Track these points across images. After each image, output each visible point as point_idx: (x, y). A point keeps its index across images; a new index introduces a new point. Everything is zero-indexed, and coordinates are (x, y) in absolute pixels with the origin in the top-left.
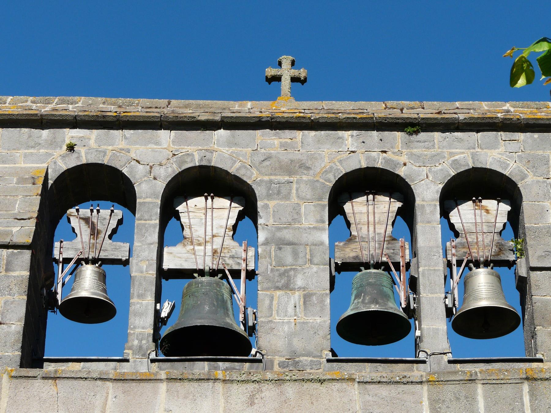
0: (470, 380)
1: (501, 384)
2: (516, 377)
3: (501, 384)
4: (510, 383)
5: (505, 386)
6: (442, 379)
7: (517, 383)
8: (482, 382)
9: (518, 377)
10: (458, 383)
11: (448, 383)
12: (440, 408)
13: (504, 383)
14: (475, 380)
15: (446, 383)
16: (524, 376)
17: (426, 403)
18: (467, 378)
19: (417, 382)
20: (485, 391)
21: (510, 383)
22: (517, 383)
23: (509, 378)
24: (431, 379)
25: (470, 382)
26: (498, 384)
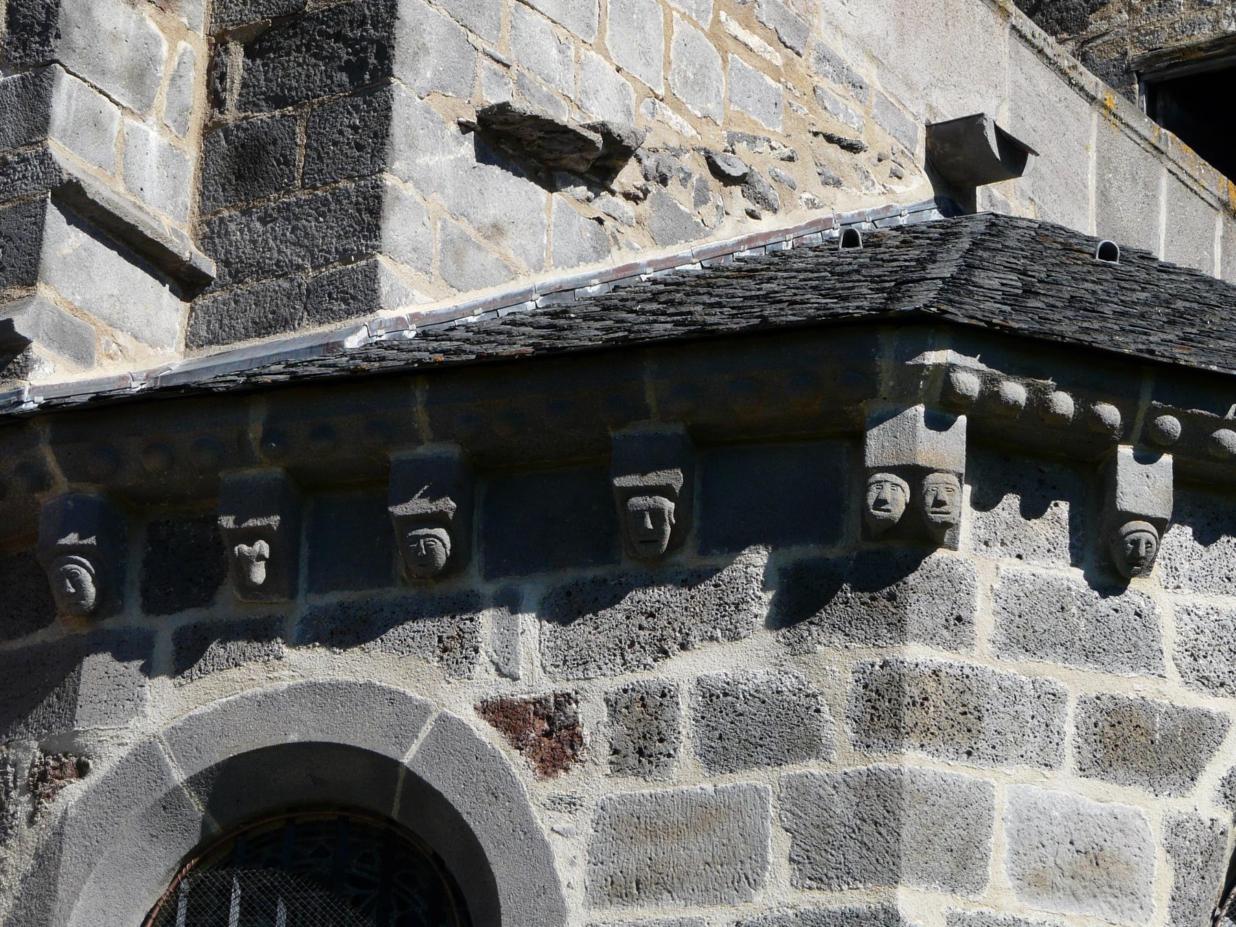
0: (1156, 148)
1: (1192, 190)
2: (1213, 189)
3: (1192, 190)
4: (1203, 199)
5: (1196, 199)
6: (1122, 115)
7: (1212, 206)
8: (1170, 165)
9: (1216, 192)
10: (1139, 141)
11: (1127, 131)
12: (1109, 181)
13: (1196, 193)
14: (1162, 153)
15: (1122, 127)
16: (1225, 198)
17: (1093, 154)
18: (1153, 141)
19: (1087, 95)
20: (1171, 191)
21: (1203, 199)
22: (1212, 206)
23: (1205, 185)
24: (1108, 103)
25: (1155, 152)
26: (1187, 186)
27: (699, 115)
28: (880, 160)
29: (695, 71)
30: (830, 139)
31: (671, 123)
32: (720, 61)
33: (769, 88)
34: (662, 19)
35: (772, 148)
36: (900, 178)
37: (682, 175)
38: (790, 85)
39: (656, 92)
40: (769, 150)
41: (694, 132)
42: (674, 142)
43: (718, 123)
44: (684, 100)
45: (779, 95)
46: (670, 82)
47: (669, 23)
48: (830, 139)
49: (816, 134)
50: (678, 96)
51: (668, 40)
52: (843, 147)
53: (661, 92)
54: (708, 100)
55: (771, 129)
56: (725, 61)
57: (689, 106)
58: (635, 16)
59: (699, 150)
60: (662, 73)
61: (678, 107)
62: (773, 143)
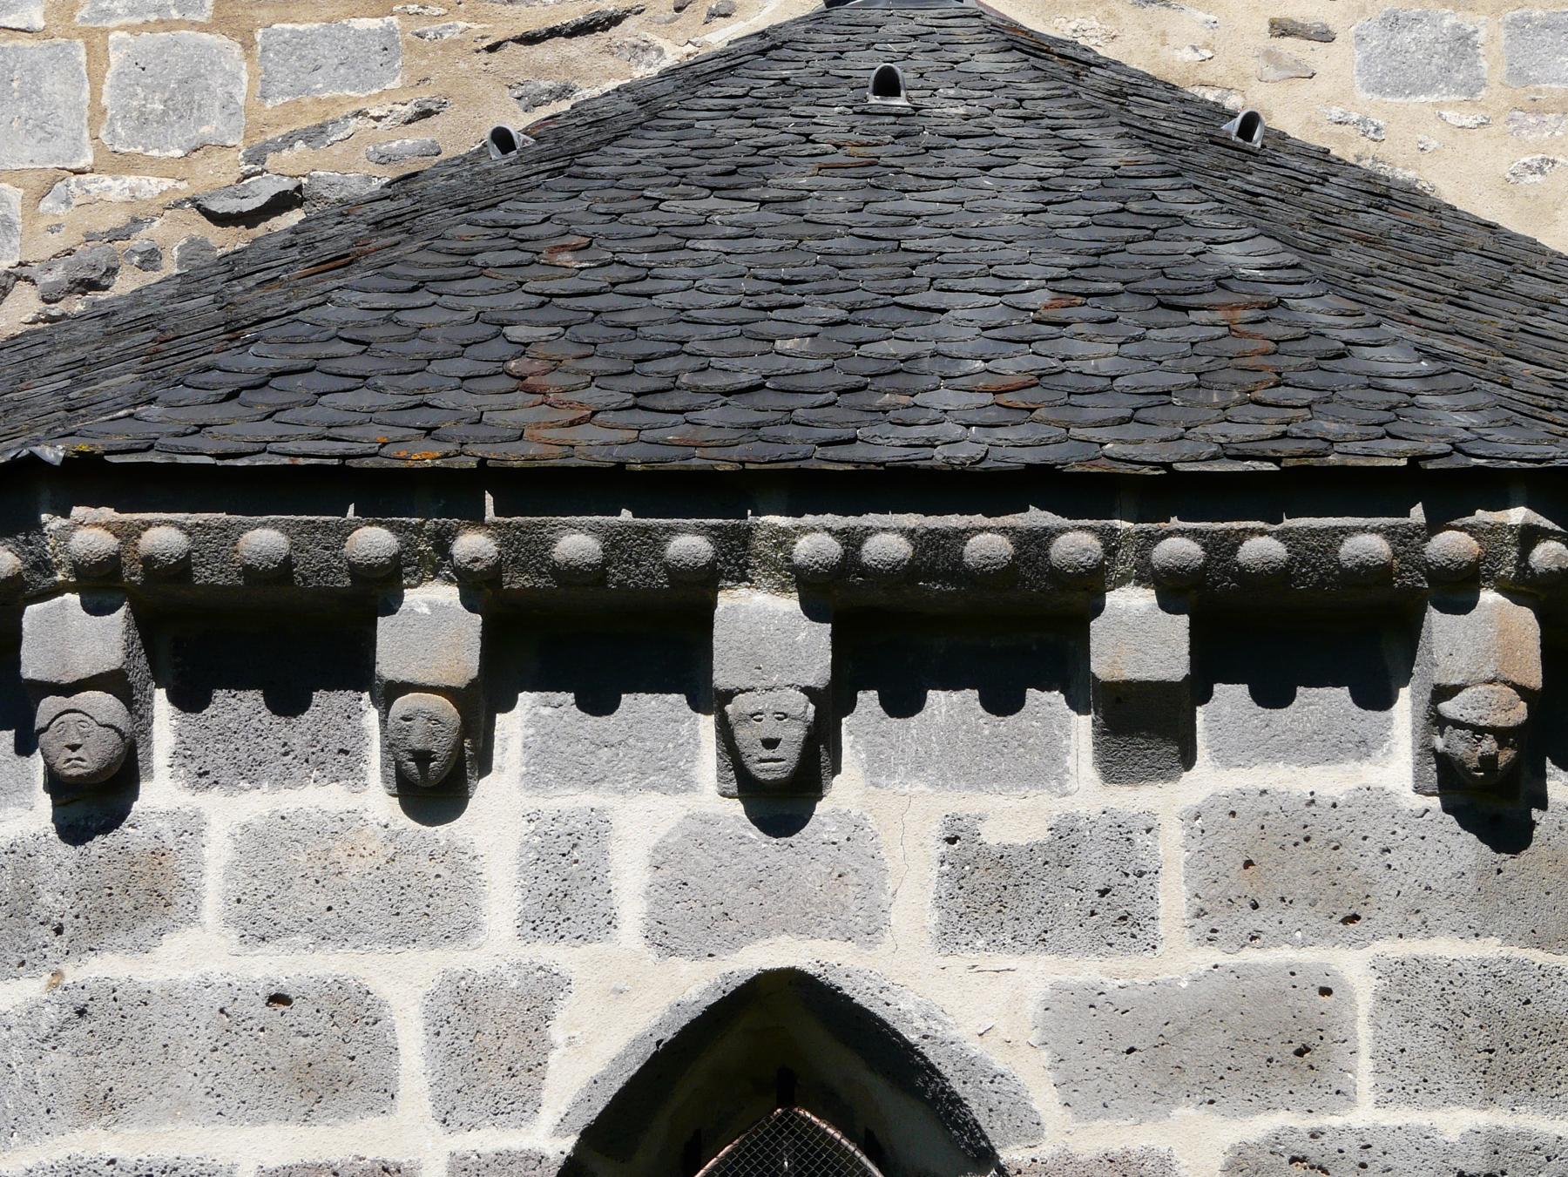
27: (179, 153)
28: (678, 10)
29: (167, 95)
30: (529, 39)
31: (111, 196)
32: (237, 50)
33: (361, 36)
34: (83, 58)
35: (378, 119)
36: (726, 16)
37: (136, 259)
38: (413, 8)
39: (74, 166)
40: (373, 123)
41: (169, 183)
42: (118, 219)
43: (229, 143)
44: (140, 149)
45: (392, 34)
46: (106, 139)
47: (97, 56)
48: (529, 39)
49: (492, 49)
50: (124, 150)
51: (96, 80)
52: (570, 35)
53: (86, 161)
54: (201, 121)
55: (376, 91)
56: (247, 46)
57: (155, 153)
58: (15, 84)
59: (178, 205)
60: (86, 134)
61: (121, 164)
62: (375, 112)
